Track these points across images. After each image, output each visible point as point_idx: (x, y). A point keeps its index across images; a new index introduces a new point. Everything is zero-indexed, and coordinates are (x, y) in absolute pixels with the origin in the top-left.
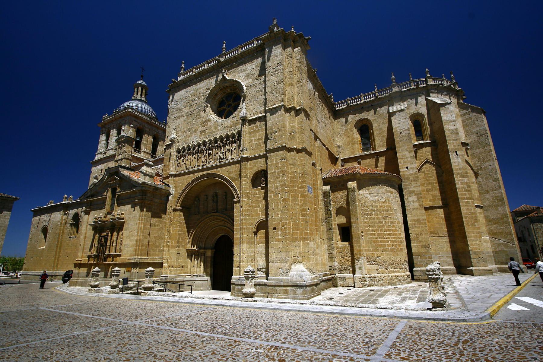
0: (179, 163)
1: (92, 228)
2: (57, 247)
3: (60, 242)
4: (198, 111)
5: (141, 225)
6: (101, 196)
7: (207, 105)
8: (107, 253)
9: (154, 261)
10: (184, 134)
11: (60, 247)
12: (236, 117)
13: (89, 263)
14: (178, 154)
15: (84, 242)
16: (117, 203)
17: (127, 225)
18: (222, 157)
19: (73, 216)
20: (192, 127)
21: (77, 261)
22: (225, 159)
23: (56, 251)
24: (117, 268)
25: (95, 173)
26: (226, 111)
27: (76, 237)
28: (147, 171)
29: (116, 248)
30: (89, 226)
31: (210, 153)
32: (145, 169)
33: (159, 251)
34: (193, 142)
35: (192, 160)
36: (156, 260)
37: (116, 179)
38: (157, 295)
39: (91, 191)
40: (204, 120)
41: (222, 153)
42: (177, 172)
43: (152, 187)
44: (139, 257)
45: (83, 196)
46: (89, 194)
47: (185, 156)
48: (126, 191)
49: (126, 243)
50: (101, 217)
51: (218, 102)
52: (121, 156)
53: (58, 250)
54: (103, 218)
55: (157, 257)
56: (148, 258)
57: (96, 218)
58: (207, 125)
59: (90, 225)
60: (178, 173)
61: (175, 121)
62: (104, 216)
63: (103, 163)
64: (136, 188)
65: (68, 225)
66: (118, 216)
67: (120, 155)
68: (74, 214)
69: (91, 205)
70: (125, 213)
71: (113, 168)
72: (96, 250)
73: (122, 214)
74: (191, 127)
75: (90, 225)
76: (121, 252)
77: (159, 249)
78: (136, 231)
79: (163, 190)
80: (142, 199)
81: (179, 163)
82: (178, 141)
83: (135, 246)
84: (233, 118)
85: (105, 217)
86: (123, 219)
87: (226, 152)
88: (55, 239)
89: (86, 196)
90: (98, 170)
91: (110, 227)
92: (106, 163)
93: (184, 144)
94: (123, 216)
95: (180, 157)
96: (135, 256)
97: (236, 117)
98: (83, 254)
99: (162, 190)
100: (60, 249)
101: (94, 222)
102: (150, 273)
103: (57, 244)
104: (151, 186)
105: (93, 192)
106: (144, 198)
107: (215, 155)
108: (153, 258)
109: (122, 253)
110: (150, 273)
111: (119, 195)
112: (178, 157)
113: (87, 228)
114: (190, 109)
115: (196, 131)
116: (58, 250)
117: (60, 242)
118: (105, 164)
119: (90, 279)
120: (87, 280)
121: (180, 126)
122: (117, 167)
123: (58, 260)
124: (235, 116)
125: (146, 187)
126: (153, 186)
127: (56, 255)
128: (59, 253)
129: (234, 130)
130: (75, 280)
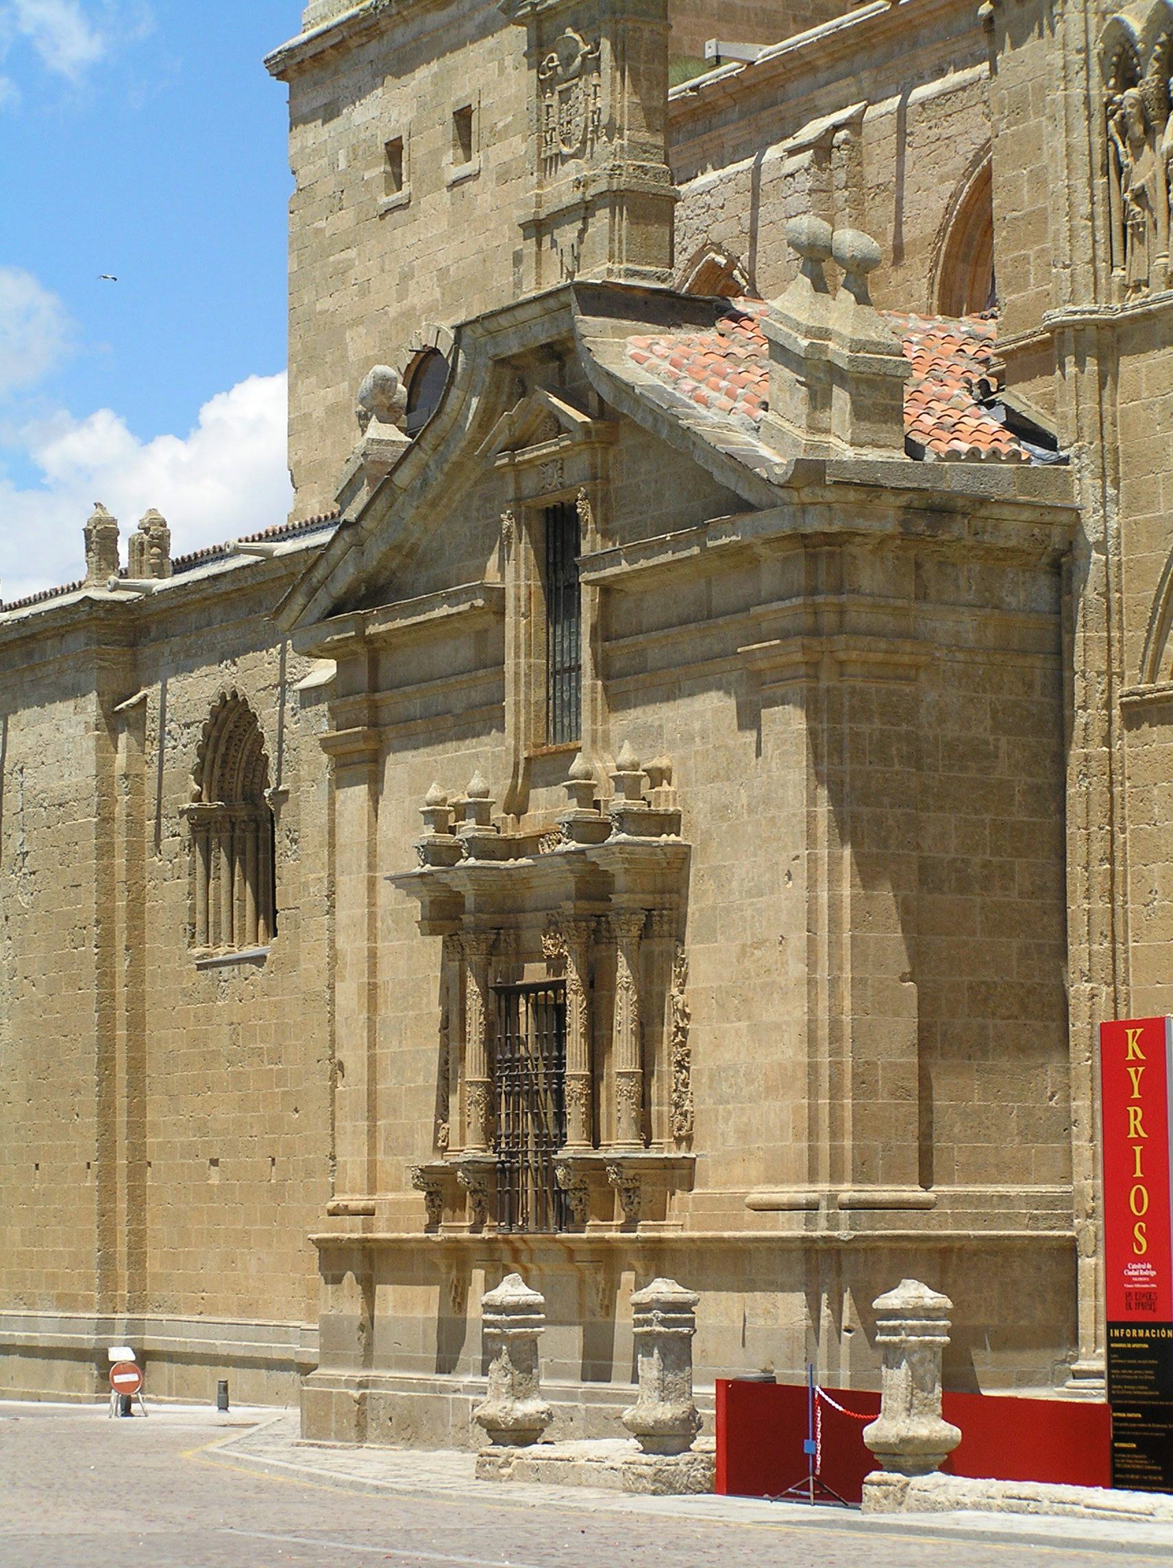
0: (1140, 196)
1: (414, 907)
2: (106, 1062)
5: (834, 881)
6: (451, 599)
8: (575, 1146)
9: (988, 1221)
11: (137, 1066)
13: (440, 1235)
15: (372, 1044)
16: (603, 670)
17: (710, 885)
19: (197, 732)
21: (332, 1213)
23: (106, 1108)
24: (664, 1288)
25: (328, 186)
27: (259, 960)
28: (825, 334)
29: (644, 1102)
30: (387, 893)
32: (803, 318)
33: (1028, 1133)
36: (1010, 1220)
37: (557, 426)
38: (976, 1507)
39: (359, 544)
42: (1134, 300)
43: (889, 498)
44: (848, 1191)
45: (300, 600)
46: (344, 579)
48: (662, 547)
49: (727, 1056)
50: (480, 811)
52: (571, 170)
53: (121, 1102)
54: (497, 814)
55: (1014, 1190)
56: (923, 1195)
57: (436, 817)
59: (399, 881)
60: (1134, 303)
62: (500, 790)
63: (403, 64)
64: (747, 520)
65: (177, 832)
66: (620, 802)
67: (565, 158)
68: (204, 713)
69: (374, 688)
70: (683, 761)
71: (521, 314)
72: (476, 1117)
73: (658, 776)
75: (399, 881)
76: (689, 1139)
77: (1027, 1113)
78: (798, 939)
79: (1006, 512)
80: (815, 632)
81: (1140, 196)
83: (802, 1082)
85: (517, 806)
86: (671, 822)
88: (73, 982)
89: (324, 600)
90: (354, 154)
91: (569, 907)
92: (434, 66)
94: (665, 799)
95: (1138, 129)
96: (813, 1177)
98: (372, 1149)
99: (996, 511)
100: (137, 1086)
101: (431, 853)
102: (912, 1331)
103: (106, 1042)
104: (873, 488)
105: (376, 551)
106: (829, 620)
108: (982, 1200)
109: (703, 1152)
110: (912, 1331)
111: (607, 589)
112: (1123, 130)
113: (372, 904)
116: (121, 1102)
118: (424, 74)
119: (467, 1379)
120: (444, 1389)
122: (551, 303)
123: (137, 1198)
125: (829, 506)
126: (897, 491)
127: (107, 1150)
128: (137, 1128)
130: (348, 1383)
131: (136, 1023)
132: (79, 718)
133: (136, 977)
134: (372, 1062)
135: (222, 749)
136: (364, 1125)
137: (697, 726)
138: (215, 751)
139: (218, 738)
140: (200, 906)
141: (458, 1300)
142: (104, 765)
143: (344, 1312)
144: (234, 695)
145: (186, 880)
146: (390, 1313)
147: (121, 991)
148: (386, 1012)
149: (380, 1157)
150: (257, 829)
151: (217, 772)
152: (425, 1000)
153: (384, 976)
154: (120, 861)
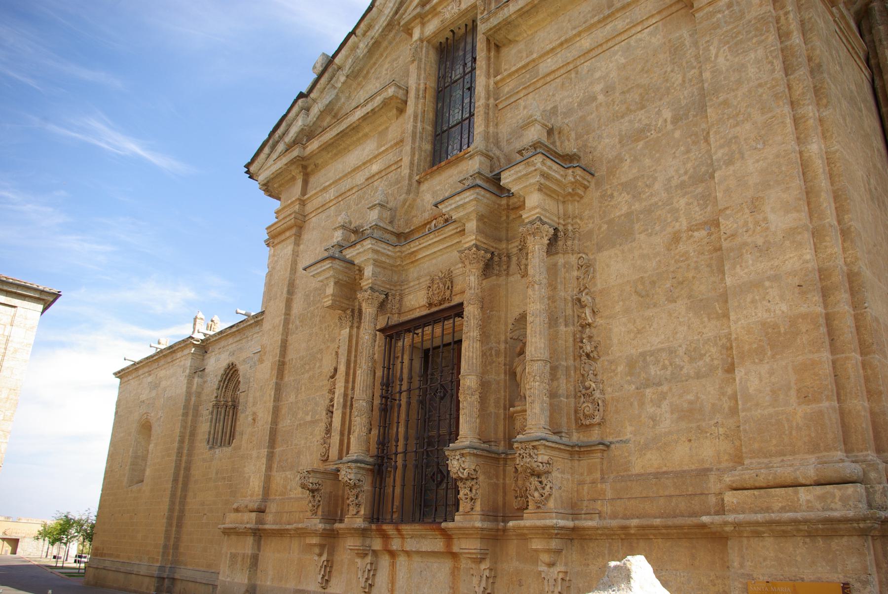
3: (183, 465)
89: (281, 147)
98: (269, 468)
117: (183, 465)
131: (188, 469)
132: (185, 374)
133: (190, 455)
134: (276, 412)
135: (226, 383)
136: (264, 451)
137: (598, 88)
138: (224, 383)
139: (225, 379)
140: (212, 432)
141: (326, 578)
142: (189, 387)
143: (236, 580)
144: (232, 364)
145: (209, 424)
146: (268, 583)
147: (184, 458)
148: (288, 378)
149: (274, 473)
150: (234, 408)
151: (224, 390)
152: (318, 365)
153: (291, 355)
154: (190, 418)
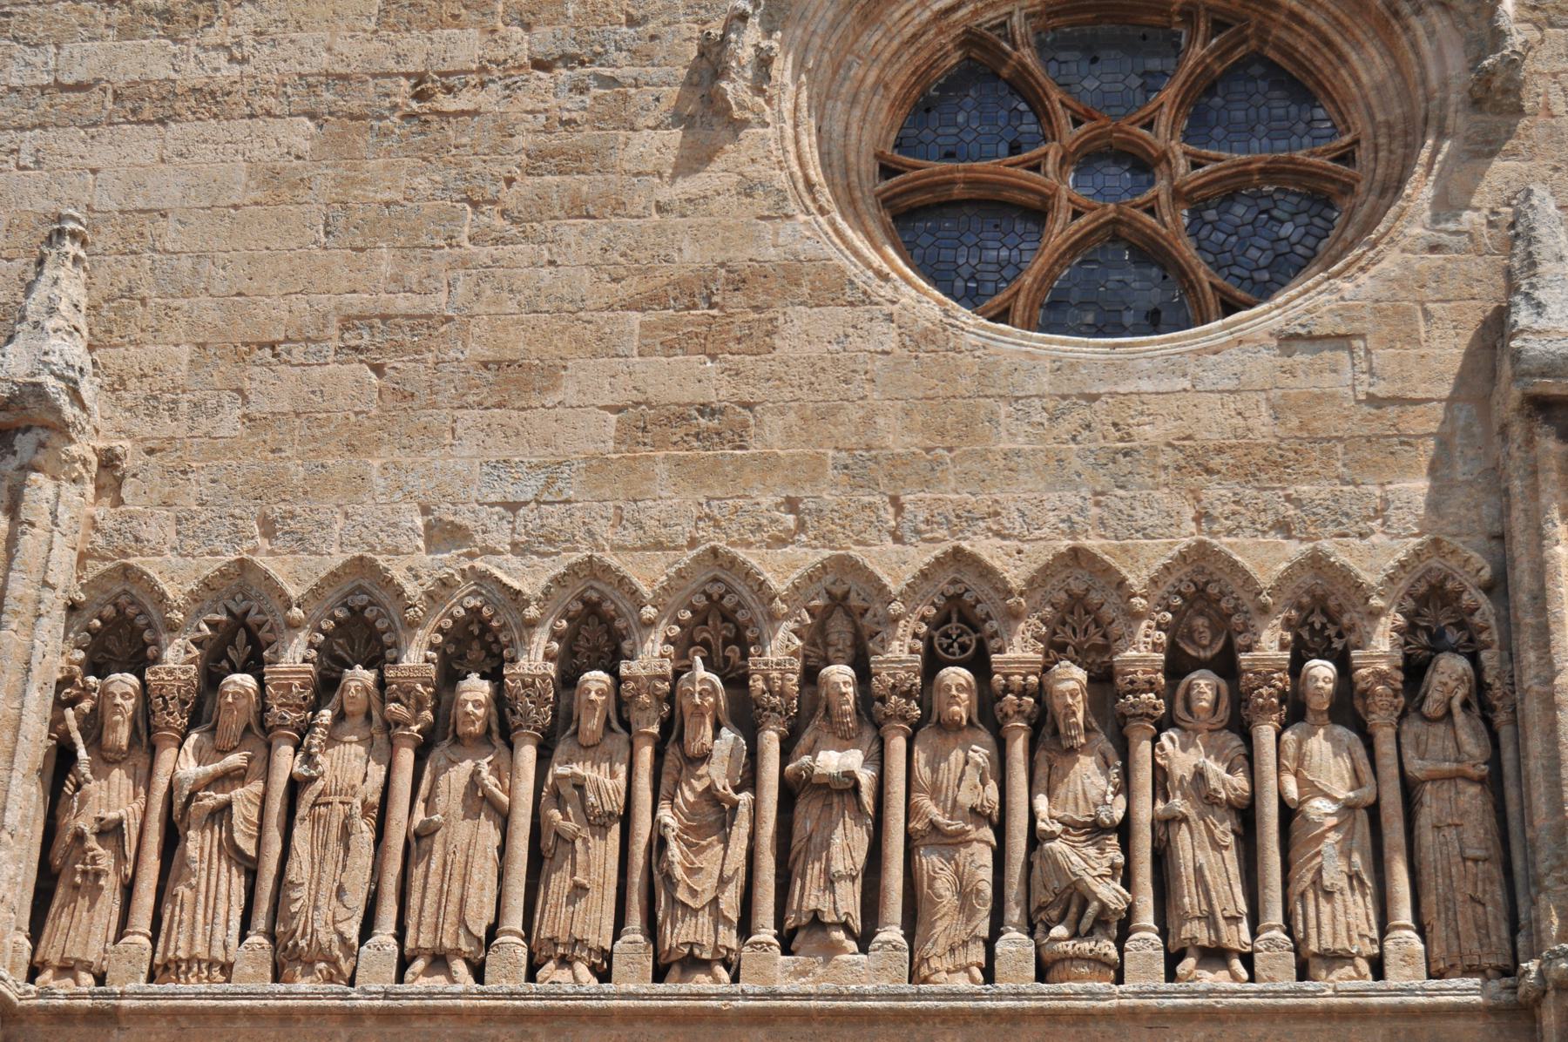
4: (571, 105)
7: (764, 62)
10: (256, 377)
12: (1341, 340)
14: (98, 666)
18: (1109, 892)
20: (438, 302)
22: (1146, 942)
26: (1060, 230)
31: (847, 787)
34: (443, 534)
35: (418, 842)
40: (691, 256)
41: (1095, 830)
47: (261, 730)
51: (900, 75)
58: (762, 339)
61: (70, 141)
74: (402, 303)
81: (111, 832)
82: (109, 461)
84: (1288, 340)
87: (1165, 825)
93: (237, 535)
95: (122, 735)
97: (1341, 340)
107: (950, 842)
114: (405, 41)
115: (524, 387)
121: (170, 234)
124: (1326, 326)
129: (1339, 519)
